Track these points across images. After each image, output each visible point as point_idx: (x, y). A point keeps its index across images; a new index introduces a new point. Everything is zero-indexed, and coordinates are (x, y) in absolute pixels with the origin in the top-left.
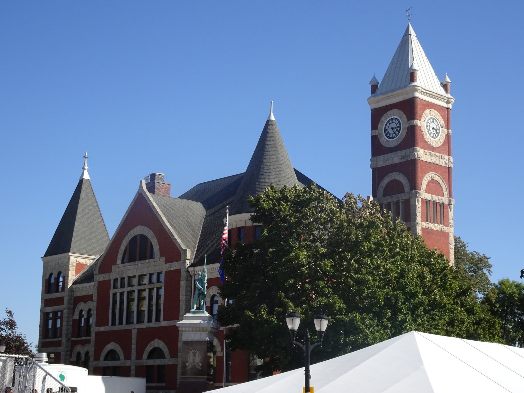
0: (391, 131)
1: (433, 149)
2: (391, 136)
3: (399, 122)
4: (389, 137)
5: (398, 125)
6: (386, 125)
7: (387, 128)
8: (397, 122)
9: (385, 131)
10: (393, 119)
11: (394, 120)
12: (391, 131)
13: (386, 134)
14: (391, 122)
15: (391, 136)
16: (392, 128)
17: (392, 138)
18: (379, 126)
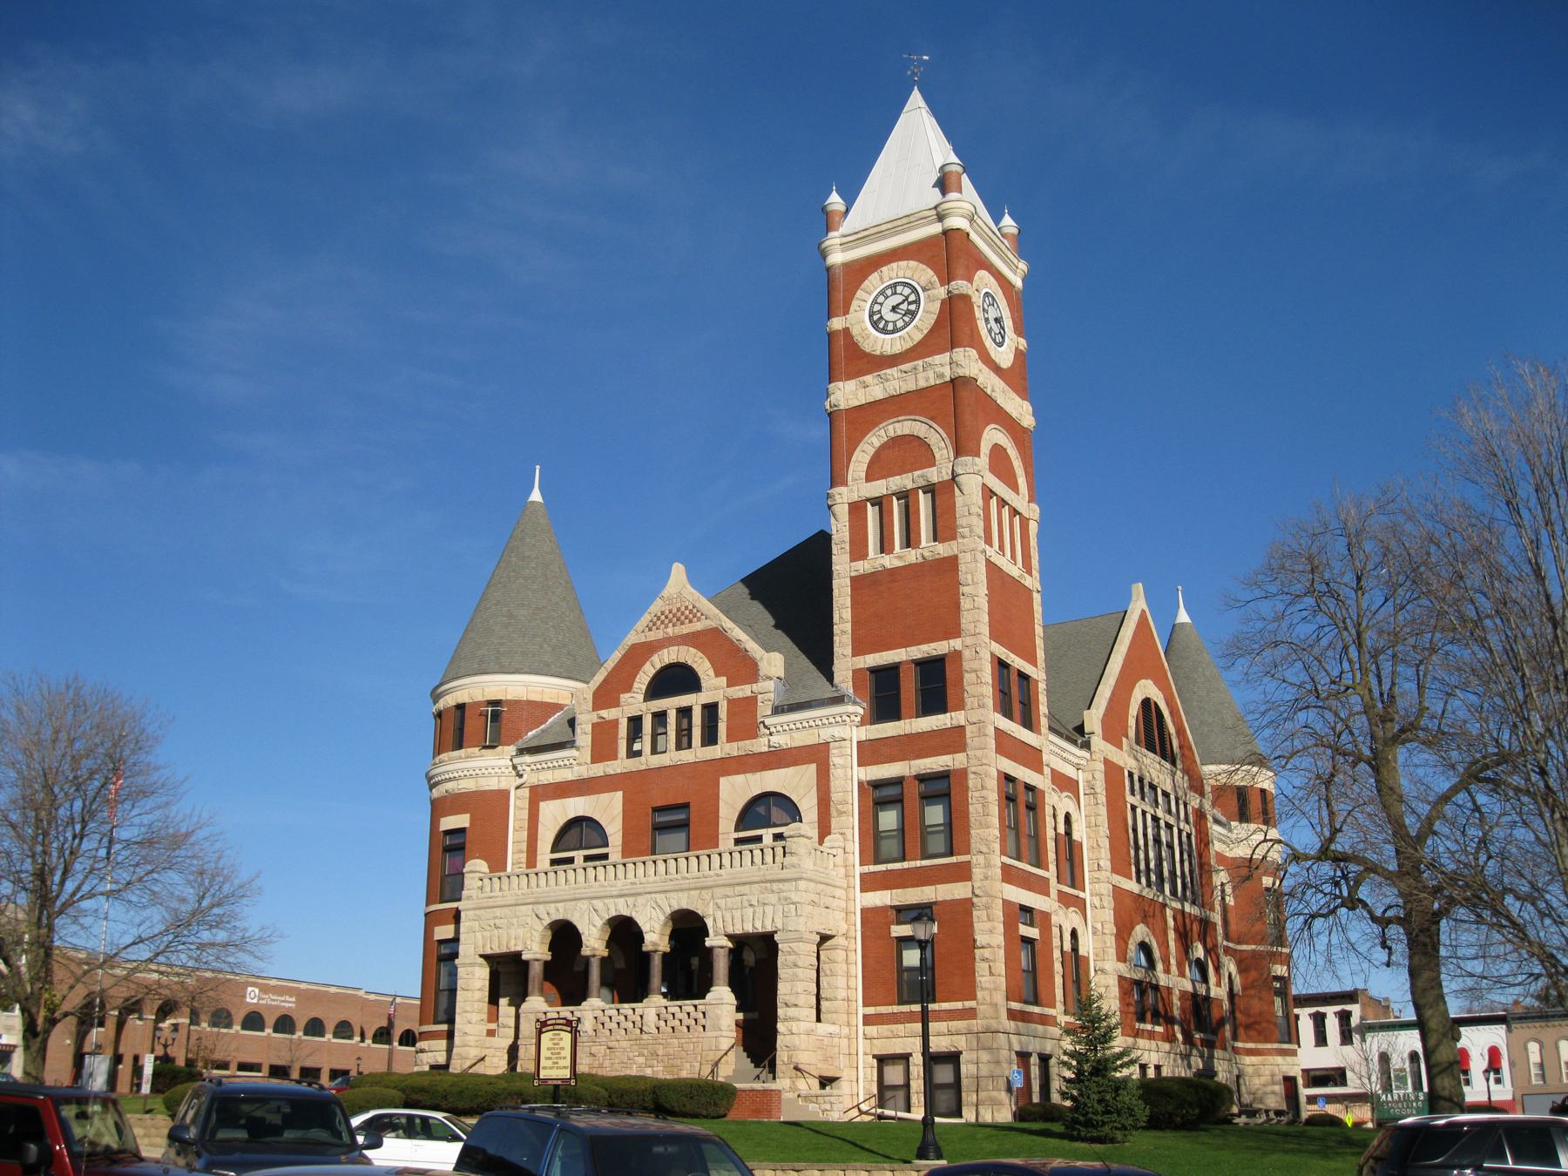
0: (890, 316)
1: (997, 369)
2: (890, 327)
3: (914, 290)
4: (884, 331)
5: (912, 298)
6: (875, 302)
7: (877, 308)
8: (907, 291)
9: (871, 316)
10: (895, 285)
11: (899, 289)
12: (890, 316)
13: (875, 324)
14: (889, 292)
15: (890, 327)
16: (894, 309)
17: (893, 332)
18: (855, 303)
